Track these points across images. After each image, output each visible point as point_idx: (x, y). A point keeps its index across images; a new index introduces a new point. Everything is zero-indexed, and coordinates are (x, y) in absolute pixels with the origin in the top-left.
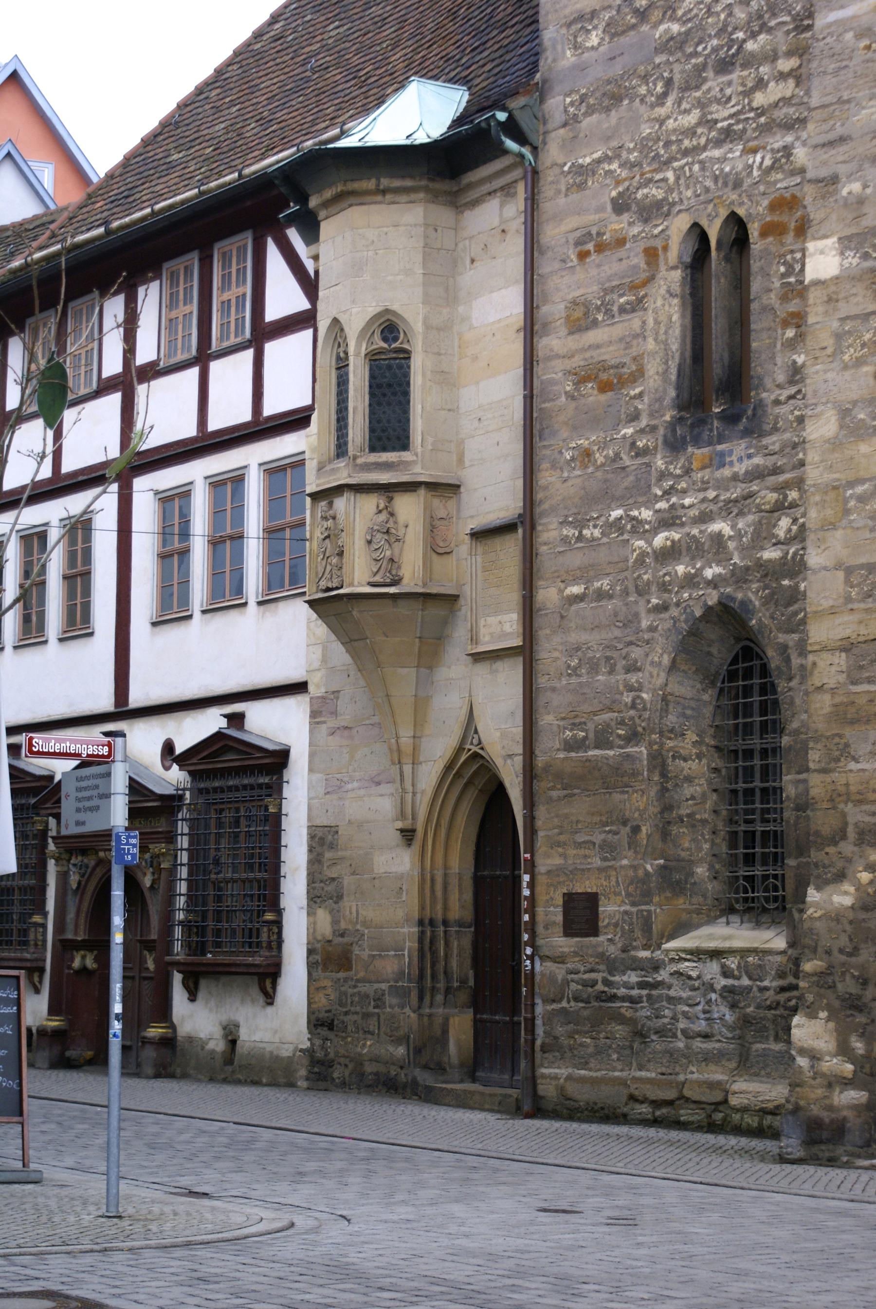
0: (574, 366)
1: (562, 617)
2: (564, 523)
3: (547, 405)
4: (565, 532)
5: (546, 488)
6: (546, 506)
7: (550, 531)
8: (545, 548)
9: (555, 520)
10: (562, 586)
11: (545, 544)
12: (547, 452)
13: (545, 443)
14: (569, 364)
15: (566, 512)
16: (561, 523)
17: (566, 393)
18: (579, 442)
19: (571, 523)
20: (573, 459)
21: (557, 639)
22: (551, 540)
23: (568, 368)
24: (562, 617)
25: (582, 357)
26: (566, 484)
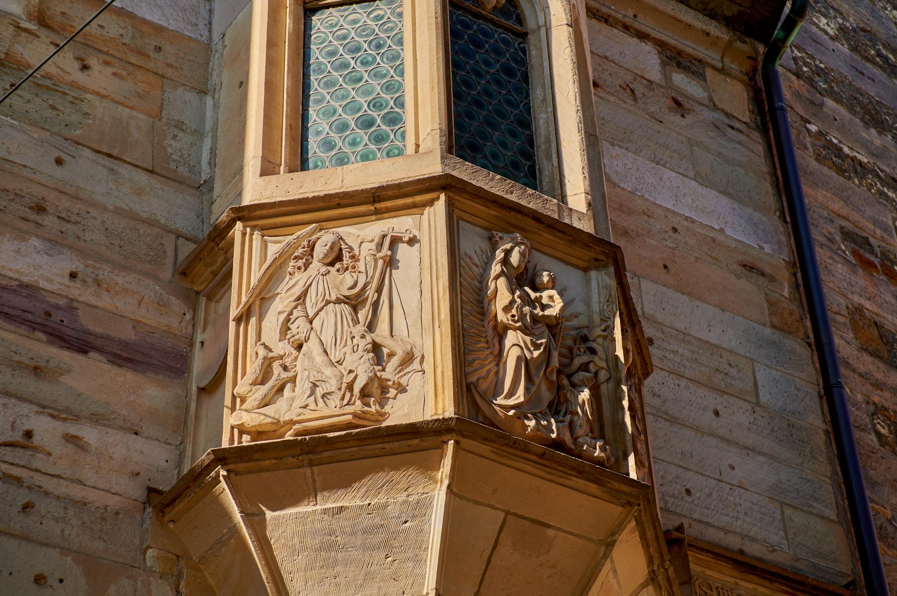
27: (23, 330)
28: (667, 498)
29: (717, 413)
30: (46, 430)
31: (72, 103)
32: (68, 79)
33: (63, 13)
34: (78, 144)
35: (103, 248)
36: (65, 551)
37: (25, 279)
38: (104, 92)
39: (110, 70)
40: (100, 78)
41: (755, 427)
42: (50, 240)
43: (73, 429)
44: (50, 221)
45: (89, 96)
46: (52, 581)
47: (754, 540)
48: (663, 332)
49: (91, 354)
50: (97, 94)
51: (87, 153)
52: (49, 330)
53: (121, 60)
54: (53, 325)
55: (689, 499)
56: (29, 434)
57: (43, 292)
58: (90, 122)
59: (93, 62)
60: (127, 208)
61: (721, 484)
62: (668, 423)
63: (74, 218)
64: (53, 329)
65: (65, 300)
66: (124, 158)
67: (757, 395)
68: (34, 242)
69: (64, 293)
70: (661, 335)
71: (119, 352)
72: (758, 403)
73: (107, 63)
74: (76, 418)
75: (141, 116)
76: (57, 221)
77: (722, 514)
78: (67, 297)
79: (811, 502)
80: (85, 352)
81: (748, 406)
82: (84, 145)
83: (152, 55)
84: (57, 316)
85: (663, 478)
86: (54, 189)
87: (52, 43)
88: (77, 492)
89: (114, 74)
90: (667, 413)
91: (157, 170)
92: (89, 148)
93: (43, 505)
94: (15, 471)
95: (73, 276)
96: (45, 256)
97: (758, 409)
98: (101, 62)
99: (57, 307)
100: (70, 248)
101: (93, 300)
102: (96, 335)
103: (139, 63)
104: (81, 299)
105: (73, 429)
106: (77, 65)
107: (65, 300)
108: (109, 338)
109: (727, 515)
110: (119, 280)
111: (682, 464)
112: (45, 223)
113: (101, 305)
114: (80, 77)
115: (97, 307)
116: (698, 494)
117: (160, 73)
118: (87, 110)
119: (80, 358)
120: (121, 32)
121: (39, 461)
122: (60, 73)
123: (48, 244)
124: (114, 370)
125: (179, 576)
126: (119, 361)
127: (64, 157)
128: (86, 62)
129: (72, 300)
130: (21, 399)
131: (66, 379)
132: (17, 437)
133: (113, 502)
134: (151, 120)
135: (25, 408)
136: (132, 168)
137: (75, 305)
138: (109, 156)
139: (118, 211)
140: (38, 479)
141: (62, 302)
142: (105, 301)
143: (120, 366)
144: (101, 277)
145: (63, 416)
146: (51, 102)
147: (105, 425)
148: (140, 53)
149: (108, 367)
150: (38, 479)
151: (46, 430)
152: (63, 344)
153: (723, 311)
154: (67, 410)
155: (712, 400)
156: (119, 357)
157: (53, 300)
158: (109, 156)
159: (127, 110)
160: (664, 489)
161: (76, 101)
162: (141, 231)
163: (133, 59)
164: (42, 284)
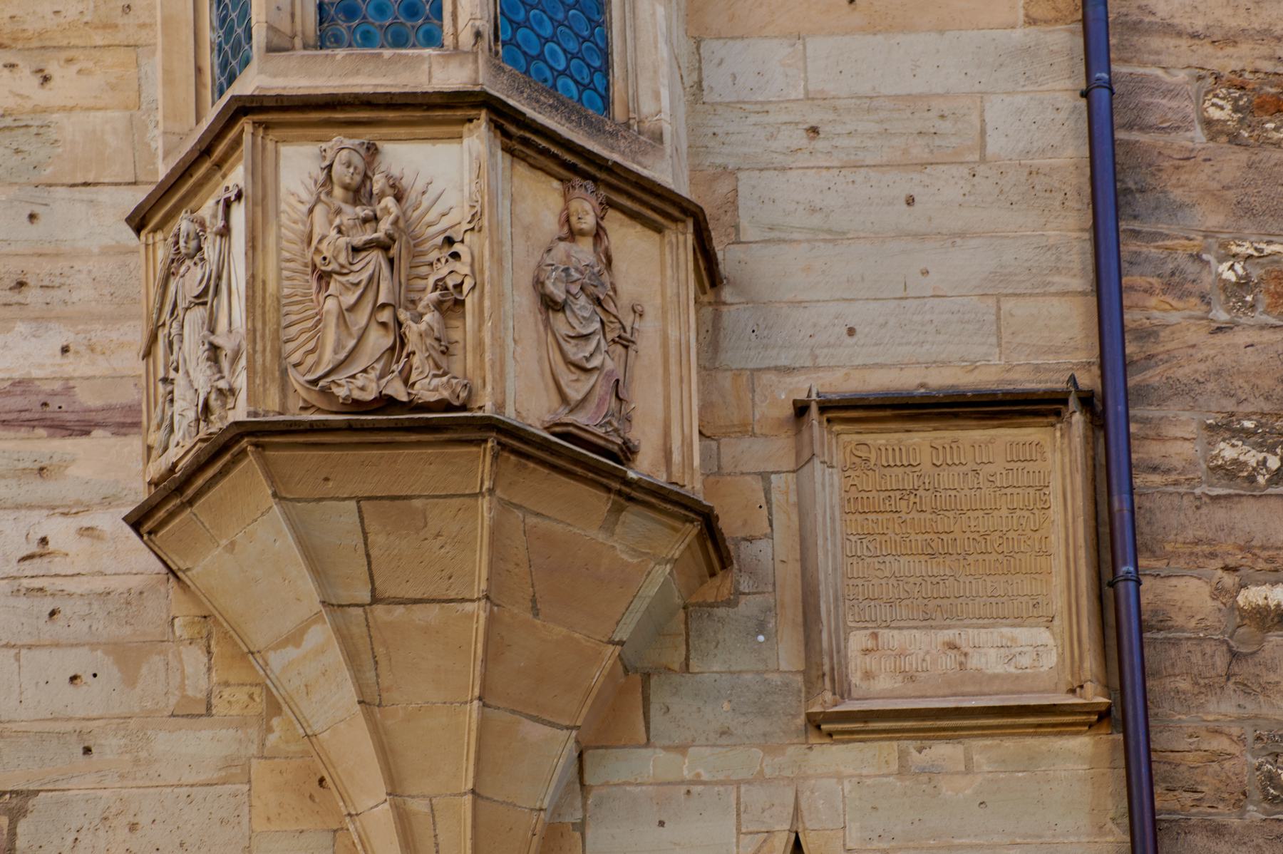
0: (1237, 65)
1: (1234, 655)
2: (1226, 428)
3: (1135, 136)
4: (1227, 451)
5: (1148, 334)
6: (1153, 376)
7: (1175, 441)
8: (1156, 479)
9: (1185, 416)
10: (1229, 580)
11: (1155, 469)
12: (1151, 250)
13: (1136, 225)
14: (1227, 61)
15: (1229, 405)
16: (1209, 427)
17: (1208, 123)
18: (1268, 249)
19: (1252, 433)
20: (1244, 284)
21: (1223, 707)
22: (1177, 462)
23: (1214, 65)
24: (1234, 655)
25: (1264, 50)
26: (1221, 339)
27: (23, 432)
28: (817, 352)
29: (910, 201)
30: (60, 531)
31: (37, 134)
32: (28, 105)
33: (12, 17)
34: (50, 185)
35: (93, 304)
36: (94, 646)
37: (17, 375)
38: (70, 103)
39: (74, 68)
40: (68, 84)
41: (972, 198)
42: (36, 319)
43: (85, 521)
44: (32, 296)
45: (55, 117)
46: (86, 677)
47: (945, 364)
48: (835, 109)
49: (97, 433)
50: (63, 109)
51: (61, 192)
52: (49, 423)
53: (84, 47)
54: (52, 416)
55: (855, 339)
56: (44, 541)
57: (37, 383)
58: (60, 150)
59: (52, 68)
60: (114, 243)
61: (903, 303)
62: (831, 245)
63: (57, 281)
64: (52, 419)
65: (60, 383)
66: (102, 180)
67: (983, 146)
68: (21, 327)
69: (58, 375)
70: (831, 116)
71: (122, 420)
72: (983, 160)
73: (69, 61)
74: (88, 508)
75: (117, 114)
76: (40, 291)
77: (900, 344)
78: (62, 378)
79: (1049, 279)
80: (87, 433)
81: (965, 171)
82: (56, 185)
83: (120, 21)
84: (54, 406)
85: (815, 325)
86: (33, 255)
87: (5, 66)
88: (99, 584)
89: (79, 72)
90: (830, 231)
91: (141, 178)
92: (63, 185)
93: (66, 608)
94: (37, 583)
95: (65, 350)
96: (33, 340)
97: (982, 170)
98: (62, 63)
99: (54, 394)
100: (58, 318)
101: (89, 371)
102: (97, 411)
103: (106, 42)
104: (76, 374)
105: (85, 521)
106: (36, 80)
107: (60, 383)
108: (109, 408)
109: (908, 343)
110: (114, 335)
111: (845, 296)
112: (28, 301)
113: (97, 373)
114: (41, 96)
115: (94, 377)
116: (867, 330)
117: (132, 42)
118: (55, 137)
119: (83, 441)
120: (80, 9)
121: (58, 566)
122: (19, 101)
123: (34, 325)
124: (120, 441)
125: (209, 637)
126: (124, 430)
127: (37, 209)
128: (46, 72)
129: (68, 379)
130: (31, 507)
131: (73, 471)
132: (34, 548)
133: (135, 582)
134: (128, 114)
135: (36, 515)
136: (114, 188)
137: (71, 383)
138: (86, 184)
139: (105, 252)
140: (59, 583)
141: (57, 386)
142: (102, 367)
143: (125, 435)
144: (94, 340)
145: (74, 511)
146: (15, 146)
147: (118, 506)
148: (105, 26)
149: (114, 440)
150: (59, 583)
151: (60, 531)
152: (65, 432)
153: (941, 32)
154: (78, 503)
155: (903, 184)
156: (123, 425)
157: (47, 387)
158: (86, 184)
159: (100, 114)
160: (813, 340)
161: (41, 131)
162: (132, 266)
163: (98, 40)
164: (36, 373)
